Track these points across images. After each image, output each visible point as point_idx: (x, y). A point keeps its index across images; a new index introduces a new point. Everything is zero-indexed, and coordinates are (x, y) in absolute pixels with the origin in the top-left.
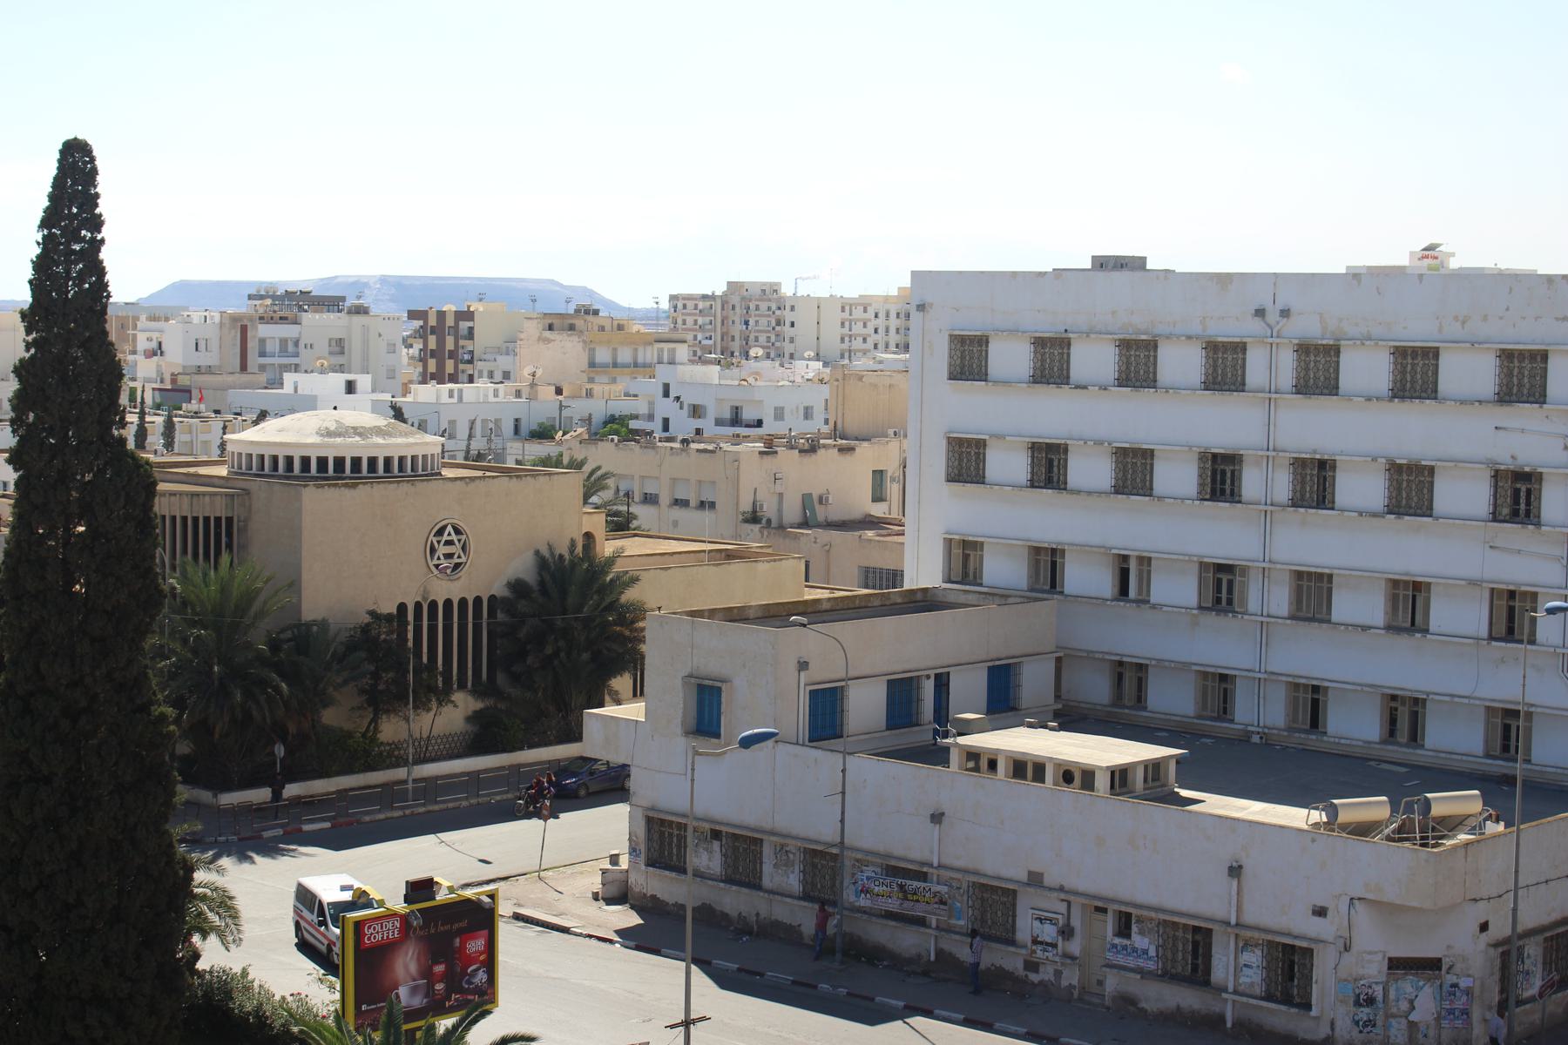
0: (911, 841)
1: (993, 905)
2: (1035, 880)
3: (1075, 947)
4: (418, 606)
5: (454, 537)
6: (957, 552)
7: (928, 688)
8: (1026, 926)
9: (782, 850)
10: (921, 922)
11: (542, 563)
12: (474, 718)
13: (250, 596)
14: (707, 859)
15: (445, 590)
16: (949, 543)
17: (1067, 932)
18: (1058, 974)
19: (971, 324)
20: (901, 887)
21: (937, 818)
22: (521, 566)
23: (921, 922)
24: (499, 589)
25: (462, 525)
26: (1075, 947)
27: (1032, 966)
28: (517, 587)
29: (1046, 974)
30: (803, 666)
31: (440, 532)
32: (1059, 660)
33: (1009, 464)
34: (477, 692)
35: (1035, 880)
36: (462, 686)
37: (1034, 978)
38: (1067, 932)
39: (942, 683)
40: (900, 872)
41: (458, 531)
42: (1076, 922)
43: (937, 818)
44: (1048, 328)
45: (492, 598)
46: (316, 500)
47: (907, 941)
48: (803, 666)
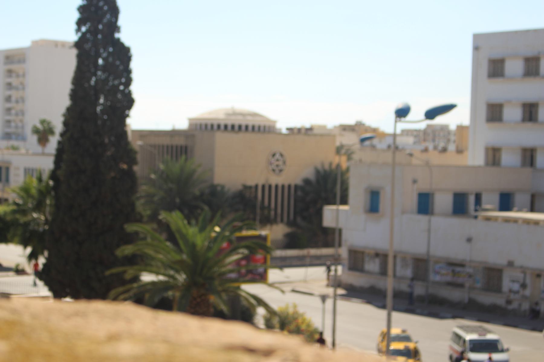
0: (457, 251)
1: (493, 276)
2: (511, 264)
3: (527, 292)
4: (263, 187)
5: (280, 158)
6: (491, 153)
7: (472, 200)
8: (507, 284)
9: (404, 259)
10: (461, 286)
11: (317, 172)
12: (287, 236)
13: (194, 171)
14: (373, 266)
15: (275, 180)
16: (487, 150)
17: (524, 286)
18: (520, 305)
19: (497, 54)
20: (453, 271)
21: (469, 240)
22: (309, 173)
23: (461, 286)
24: (298, 181)
25: (284, 153)
26: (527, 292)
27: (509, 302)
28: (307, 181)
29: (515, 305)
30: (415, 181)
31: (274, 155)
32: (533, 196)
33: (513, 113)
34: (289, 224)
35: (511, 264)
36: (282, 221)
37: (510, 307)
38: (524, 286)
39: (478, 198)
40: (454, 265)
41: (282, 155)
42: (528, 281)
43: (469, 240)
44: (530, 53)
45: (296, 187)
46: (220, 137)
47: (455, 295)
48: (415, 181)
